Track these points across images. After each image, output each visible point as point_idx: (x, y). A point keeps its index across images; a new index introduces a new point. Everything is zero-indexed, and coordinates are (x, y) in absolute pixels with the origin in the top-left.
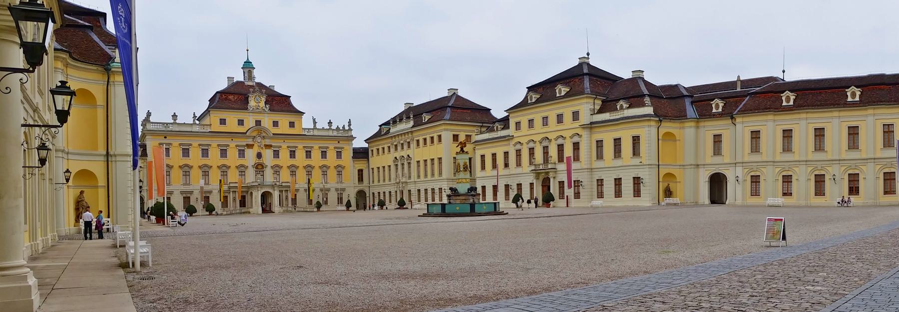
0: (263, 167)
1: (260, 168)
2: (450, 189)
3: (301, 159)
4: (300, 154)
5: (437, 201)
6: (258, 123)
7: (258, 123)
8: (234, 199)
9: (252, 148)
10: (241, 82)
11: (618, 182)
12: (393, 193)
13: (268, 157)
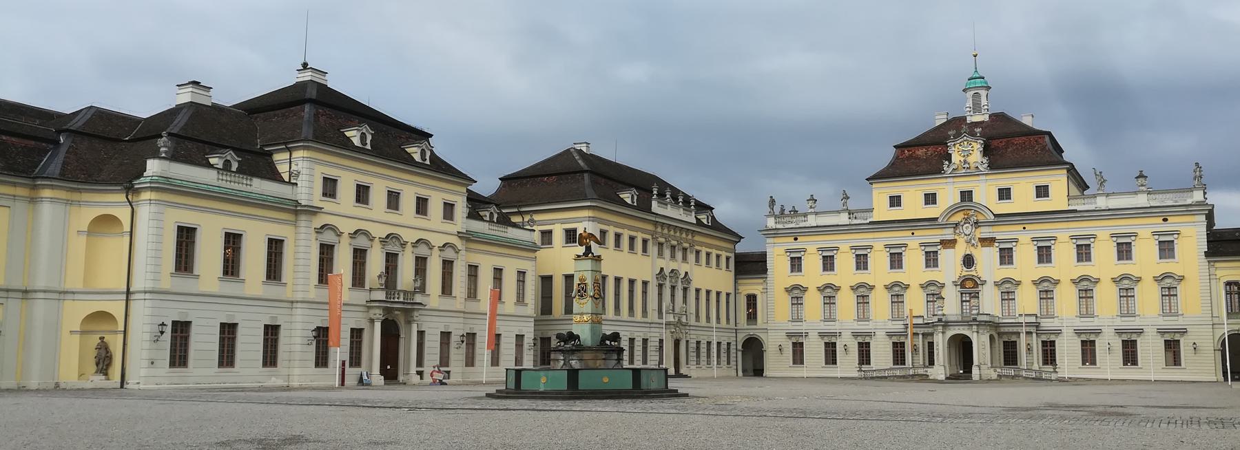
0: (976, 285)
1: (970, 287)
2: (557, 338)
3: (1064, 263)
4: (1064, 253)
5: (652, 363)
6: (966, 196)
7: (966, 196)
8: (915, 350)
9: (954, 247)
10: (964, 119)
11: (228, 331)
12: (653, 345)
13: (987, 264)
